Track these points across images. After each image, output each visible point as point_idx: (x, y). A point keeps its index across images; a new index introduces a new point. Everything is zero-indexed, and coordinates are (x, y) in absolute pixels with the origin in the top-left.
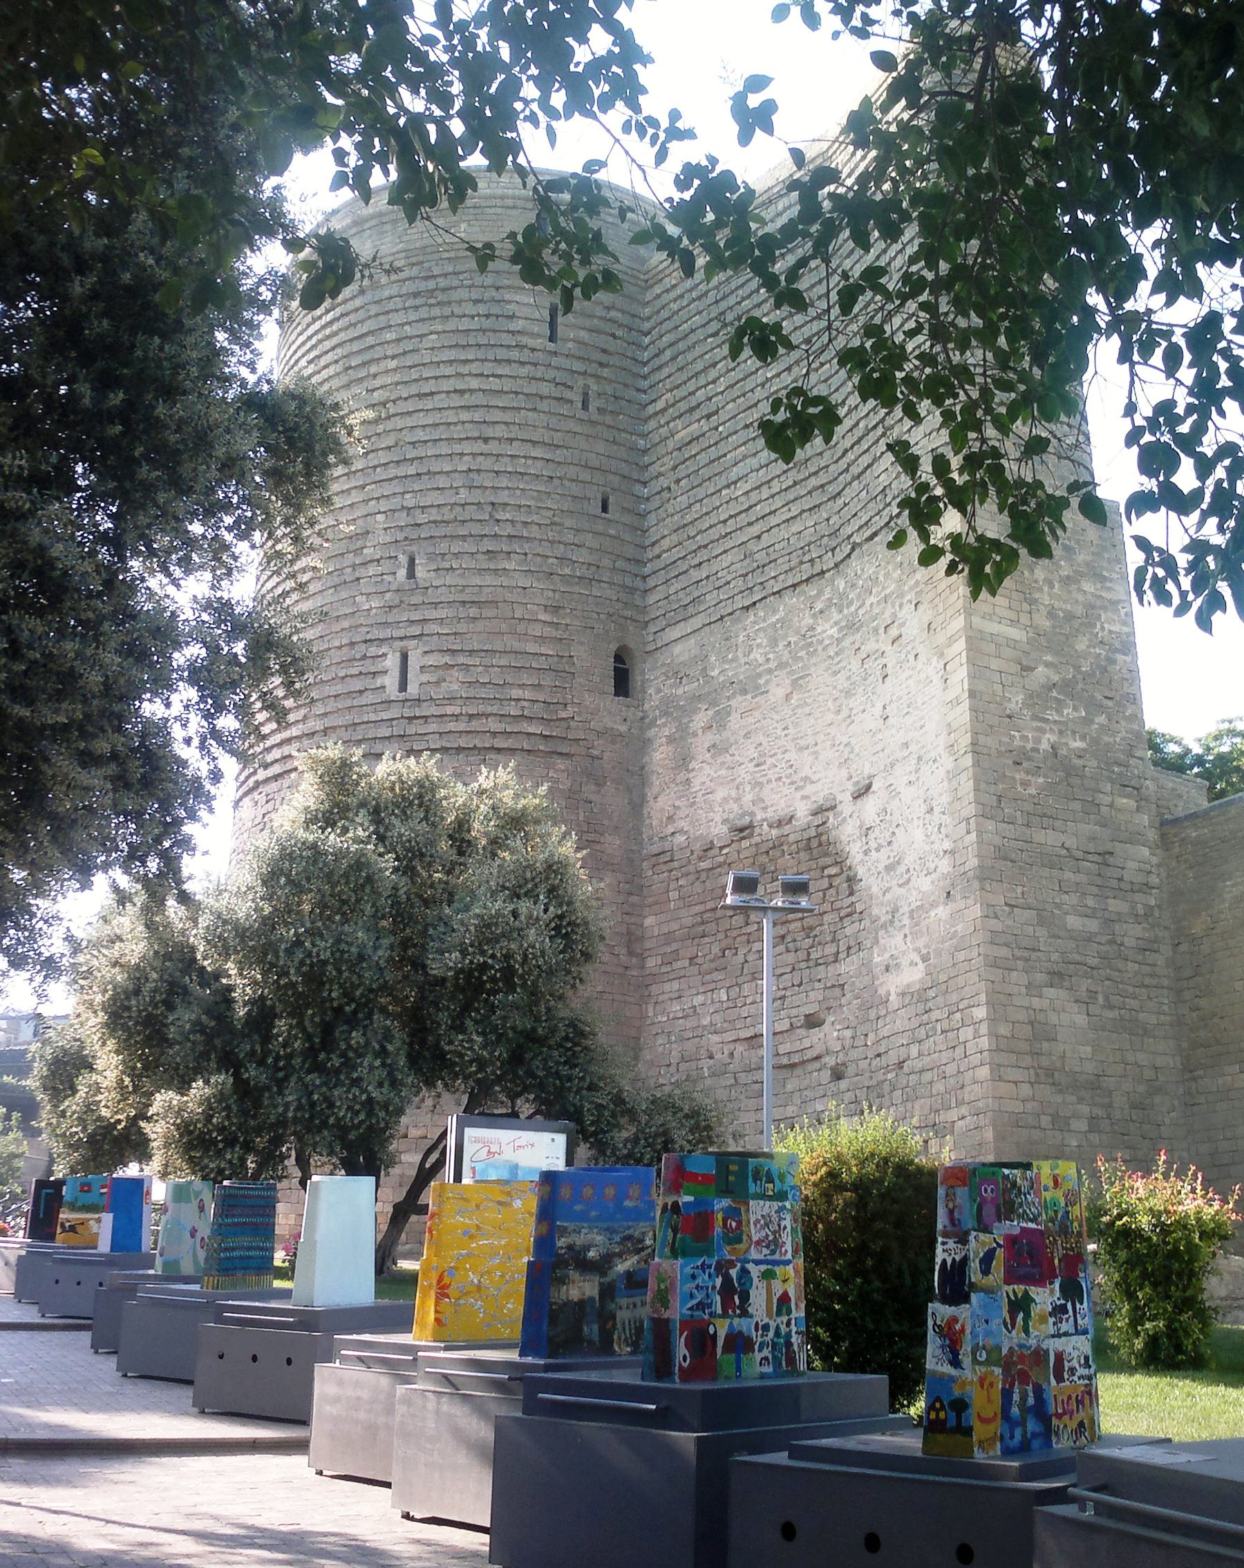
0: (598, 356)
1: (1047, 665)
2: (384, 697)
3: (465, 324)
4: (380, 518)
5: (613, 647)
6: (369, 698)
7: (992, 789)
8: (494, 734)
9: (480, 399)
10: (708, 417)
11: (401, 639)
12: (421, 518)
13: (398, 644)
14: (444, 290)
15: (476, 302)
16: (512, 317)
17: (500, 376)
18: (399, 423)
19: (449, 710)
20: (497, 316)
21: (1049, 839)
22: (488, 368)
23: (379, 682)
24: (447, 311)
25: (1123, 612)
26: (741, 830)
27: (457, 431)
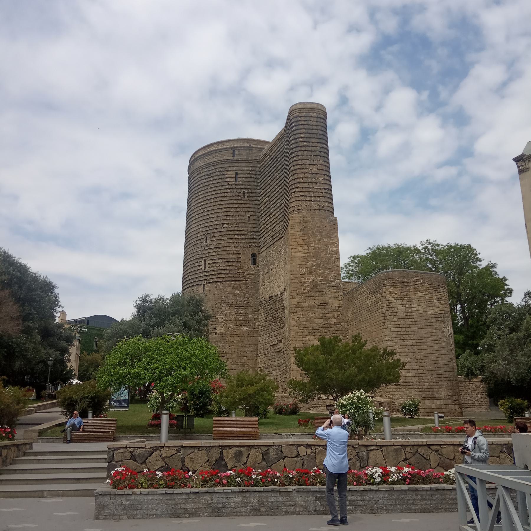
0: (247, 183)
1: (313, 261)
2: (201, 271)
3: (217, 181)
4: (201, 229)
5: (251, 253)
6: (199, 271)
7: (295, 292)
8: (223, 278)
9: (220, 199)
10: (268, 197)
11: (205, 257)
12: (208, 229)
13: (204, 258)
14: (213, 173)
15: (219, 175)
16: (227, 178)
17: (224, 193)
18: (204, 206)
19: (214, 273)
20: (224, 178)
21: (312, 301)
22: (222, 191)
23: (200, 268)
24: (213, 179)
25: (336, 245)
26: (271, 297)
27: (215, 208)
